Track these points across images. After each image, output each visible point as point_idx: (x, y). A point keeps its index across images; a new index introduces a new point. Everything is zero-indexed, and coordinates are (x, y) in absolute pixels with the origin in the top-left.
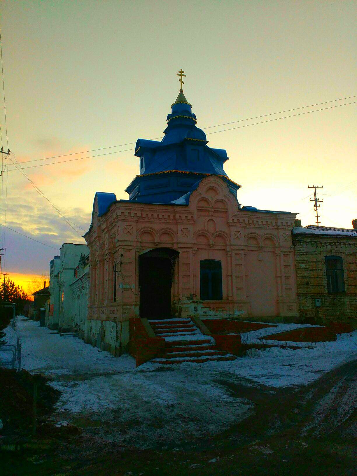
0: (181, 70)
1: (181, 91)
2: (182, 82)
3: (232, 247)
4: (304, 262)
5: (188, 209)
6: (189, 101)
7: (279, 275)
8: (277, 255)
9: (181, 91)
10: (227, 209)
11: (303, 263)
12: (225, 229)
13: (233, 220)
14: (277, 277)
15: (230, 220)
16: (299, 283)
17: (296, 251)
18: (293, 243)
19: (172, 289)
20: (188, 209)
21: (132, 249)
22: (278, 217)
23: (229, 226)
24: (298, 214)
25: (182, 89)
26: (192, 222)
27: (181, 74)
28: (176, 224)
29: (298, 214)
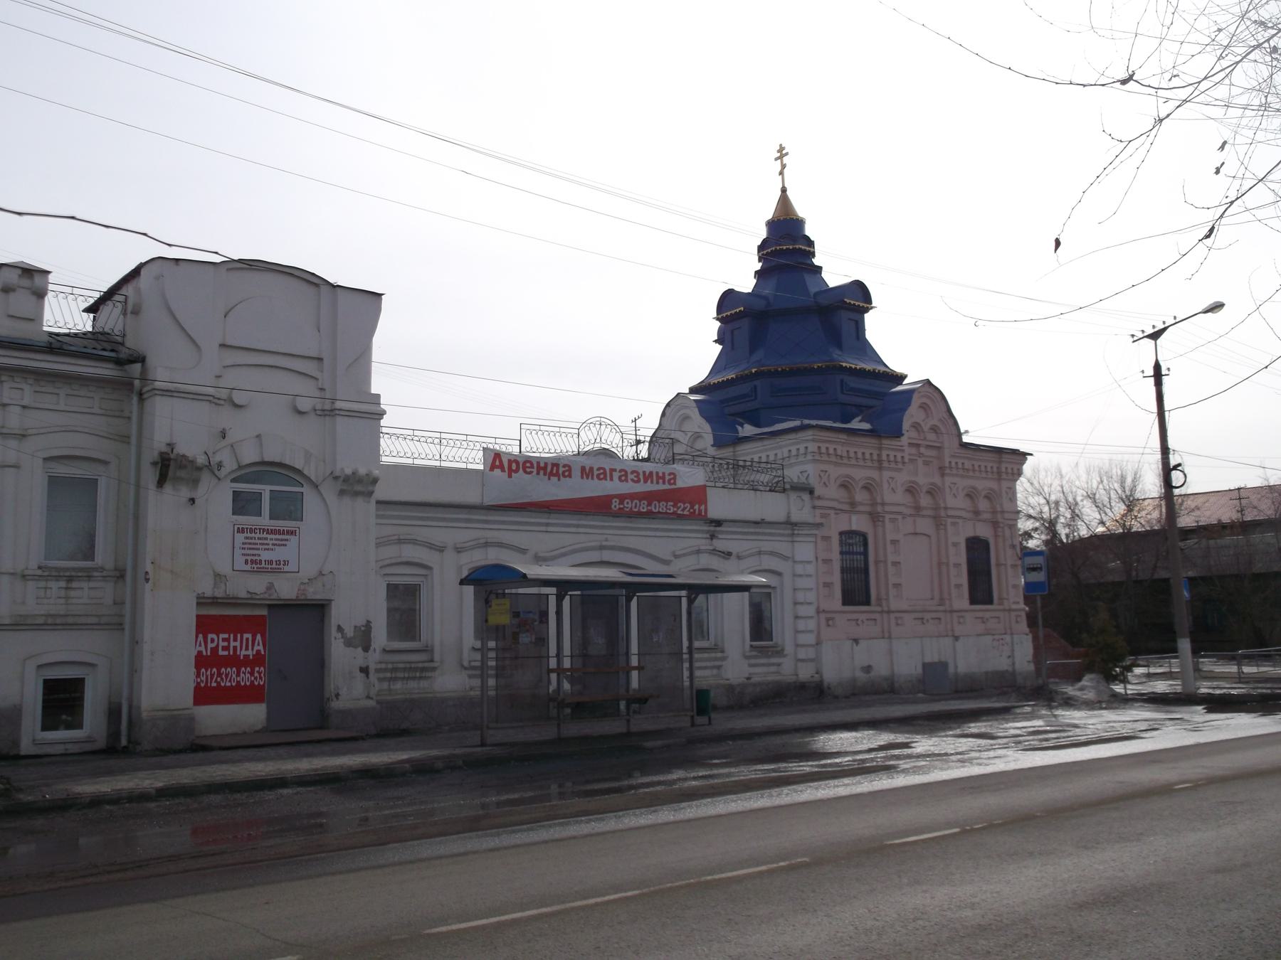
0: (781, 145)
1: (784, 190)
3: (950, 513)
5: (899, 443)
6: (801, 209)
9: (784, 190)
10: (942, 443)
12: (937, 480)
13: (950, 462)
15: (947, 465)
20: (899, 443)
22: (1003, 460)
23: (943, 475)
25: (786, 186)
26: (900, 466)
28: (880, 468)
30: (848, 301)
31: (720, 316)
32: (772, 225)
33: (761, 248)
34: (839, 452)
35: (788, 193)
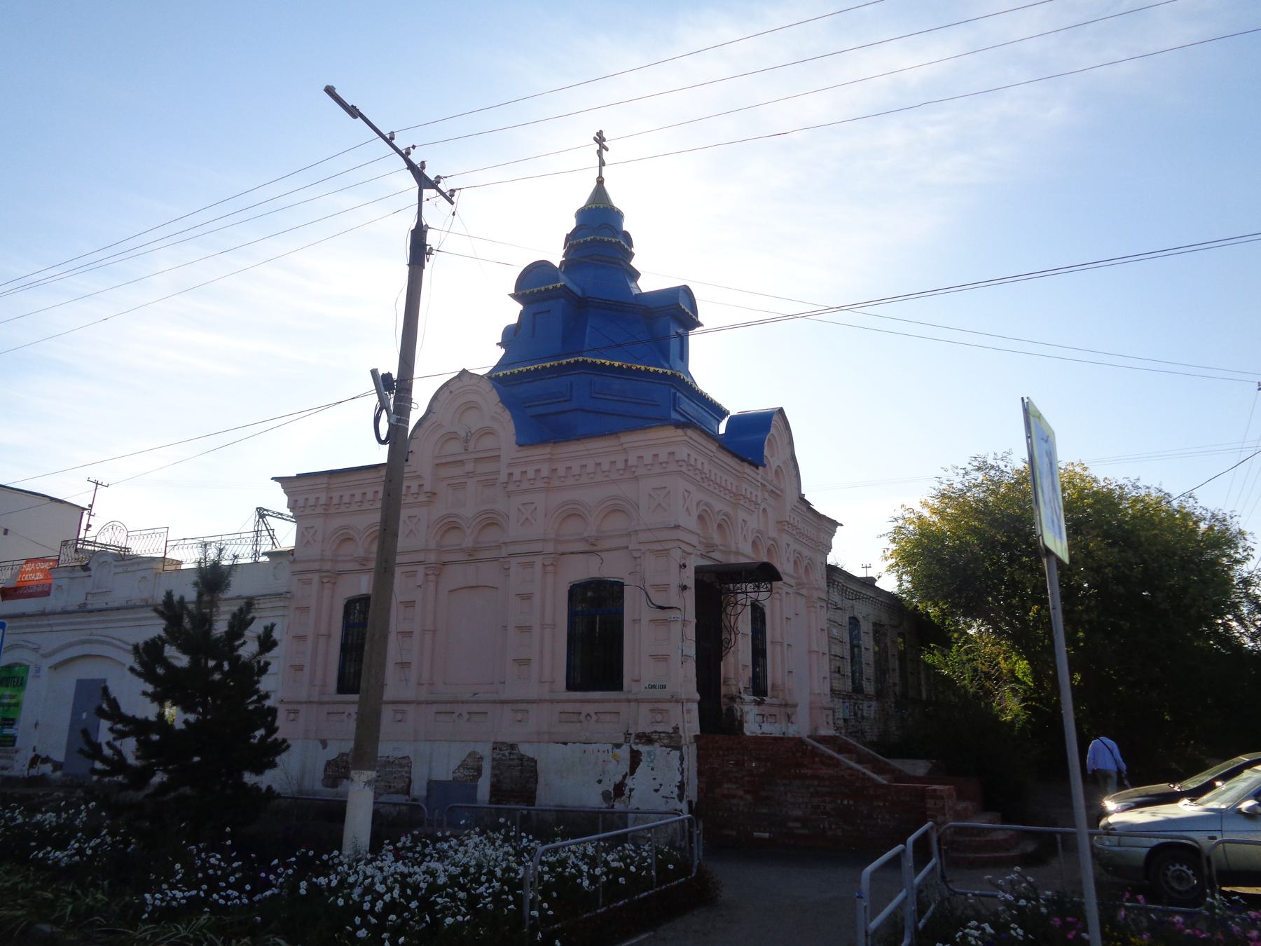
1: (600, 181)
2: (602, 163)
4: (836, 624)
7: (815, 648)
8: (813, 606)
9: (600, 181)
11: (835, 627)
14: (810, 652)
16: (832, 670)
17: (830, 602)
18: (828, 586)
19: (722, 663)
21: (691, 554)
24: (842, 525)
25: (603, 176)
27: (600, 139)
29: (842, 525)
30: (683, 307)
31: (520, 293)
32: (582, 215)
33: (569, 238)
34: (706, 470)
35: (606, 185)
